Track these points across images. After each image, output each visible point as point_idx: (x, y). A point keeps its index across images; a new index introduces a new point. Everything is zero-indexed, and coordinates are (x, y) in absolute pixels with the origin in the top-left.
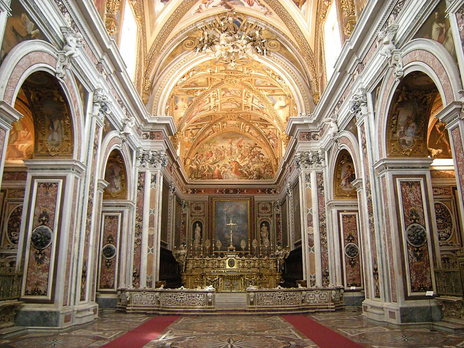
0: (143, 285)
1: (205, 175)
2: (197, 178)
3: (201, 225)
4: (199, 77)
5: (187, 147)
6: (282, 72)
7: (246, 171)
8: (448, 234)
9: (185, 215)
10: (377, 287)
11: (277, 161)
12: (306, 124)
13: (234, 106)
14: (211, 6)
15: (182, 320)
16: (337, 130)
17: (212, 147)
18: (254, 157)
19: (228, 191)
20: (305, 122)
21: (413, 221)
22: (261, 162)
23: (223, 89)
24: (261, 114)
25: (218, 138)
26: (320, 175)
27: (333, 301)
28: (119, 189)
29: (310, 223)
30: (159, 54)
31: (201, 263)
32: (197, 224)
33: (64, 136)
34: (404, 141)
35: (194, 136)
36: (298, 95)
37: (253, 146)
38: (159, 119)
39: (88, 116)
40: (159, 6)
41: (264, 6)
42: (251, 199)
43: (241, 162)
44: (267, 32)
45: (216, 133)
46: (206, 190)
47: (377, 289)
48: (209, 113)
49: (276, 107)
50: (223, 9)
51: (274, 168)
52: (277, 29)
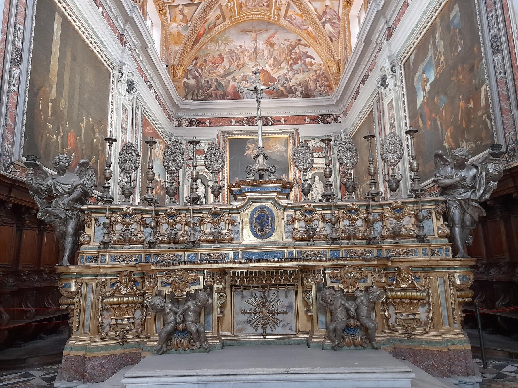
1: (211, 96)
5: (176, 43)
7: (282, 86)
17: (222, 47)
18: (295, 63)
25: (233, 31)
31: (143, 223)
35: (187, 22)
37: (293, 43)
43: (274, 70)
45: (228, 21)
51: (332, 79)
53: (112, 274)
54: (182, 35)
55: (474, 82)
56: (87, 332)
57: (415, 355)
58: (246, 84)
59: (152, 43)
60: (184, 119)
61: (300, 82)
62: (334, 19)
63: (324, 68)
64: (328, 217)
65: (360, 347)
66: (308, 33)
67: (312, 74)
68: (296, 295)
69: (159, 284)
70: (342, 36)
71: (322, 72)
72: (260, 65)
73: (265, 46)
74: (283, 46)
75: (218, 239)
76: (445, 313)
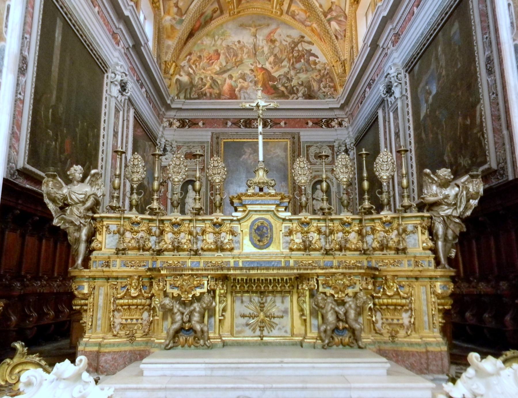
1: (205, 95)
5: (169, 37)
7: (283, 85)
17: (219, 42)
19: (250, 123)
22: (313, 69)
25: (230, 25)
31: (149, 232)
32: (190, 187)
35: (182, 15)
37: (296, 40)
42: (294, 138)
43: (275, 69)
45: (226, 16)
51: (337, 80)
53: (122, 278)
54: (176, 29)
55: (471, 100)
56: (99, 330)
57: (397, 355)
58: (243, 83)
59: (146, 41)
60: (175, 120)
61: (302, 82)
62: (340, 16)
63: (328, 68)
64: (323, 229)
65: (347, 347)
66: (313, 30)
67: (315, 74)
68: (292, 301)
69: (168, 287)
70: (348, 34)
71: (326, 72)
72: (259, 63)
73: (265, 42)
74: (284, 43)
75: (220, 248)
76: (426, 318)
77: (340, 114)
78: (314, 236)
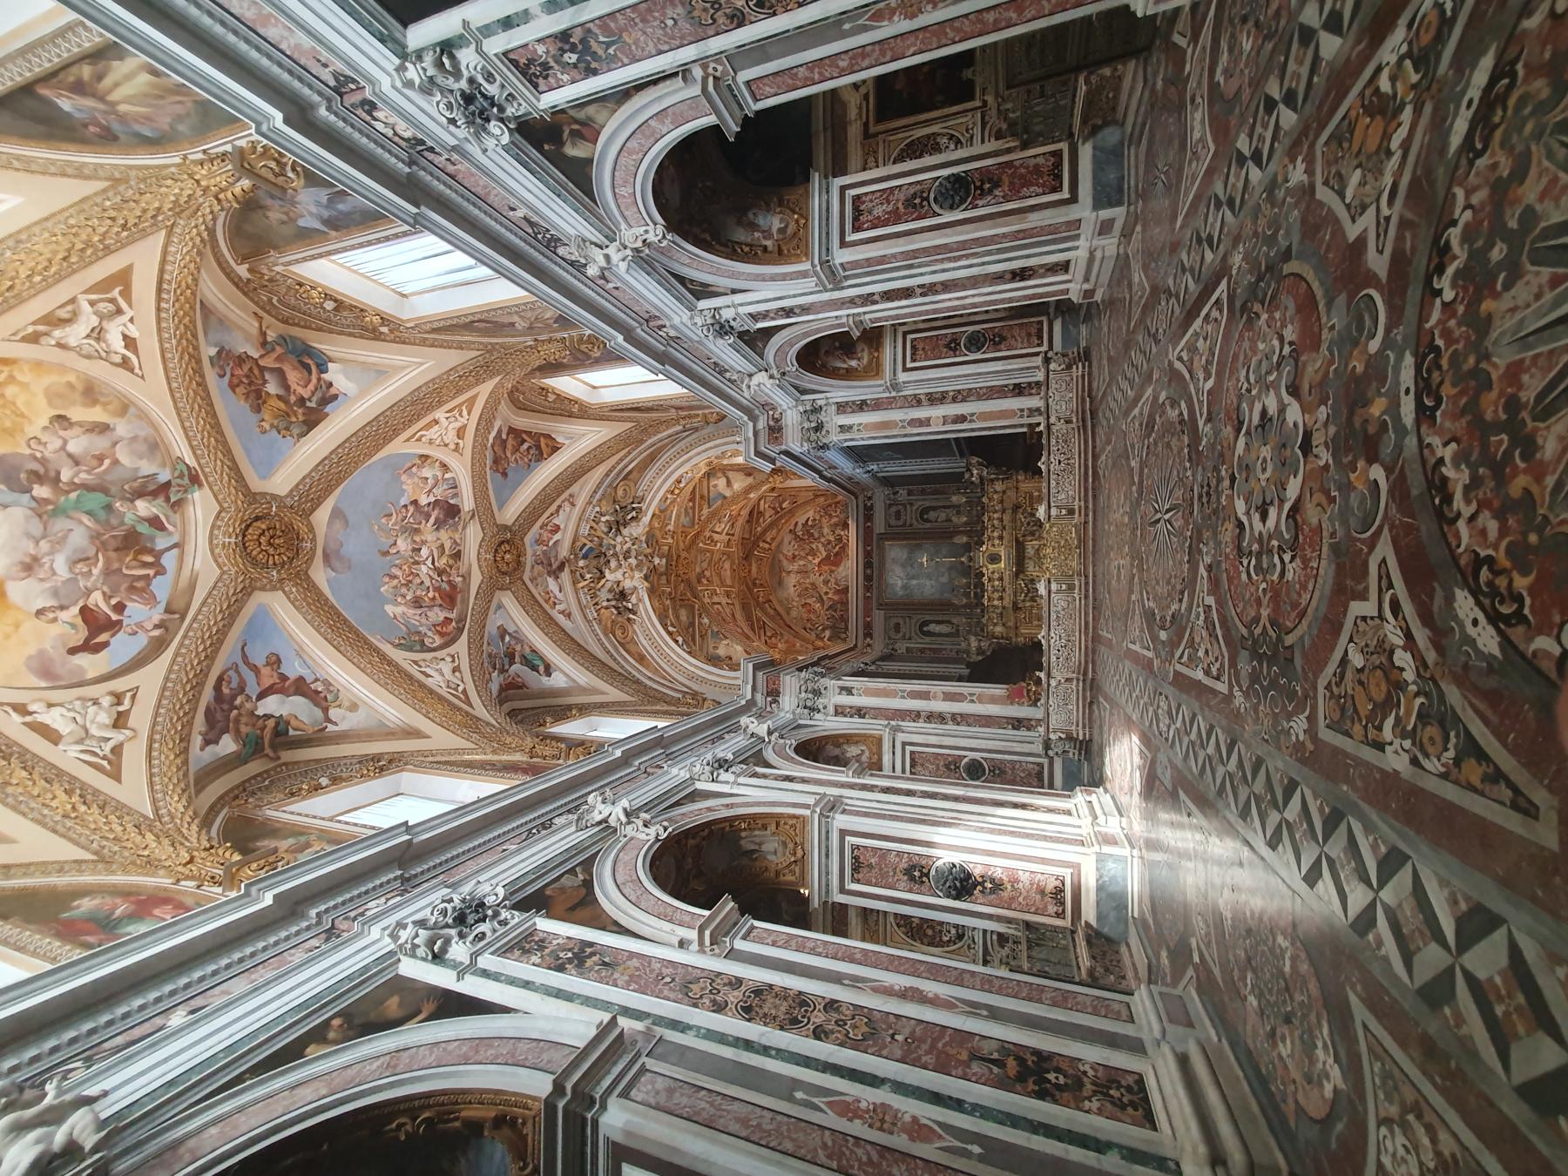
0: (1037, 713)
2: (847, 628)
3: (926, 623)
4: (677, 617)
5: (794, 645)
6: (669, 476)
8: (950, 139)
9: (907, 649)
10: (1048, 270)
11: (817, 496)
12: (756, 434)
13: (727, 565)
14: (559, 595)
15: (1105, 634)
16: (763, 373)
18: (812, 535)
20: (751, 434)
21: (925, 203)
23: (699, 582)
24: (741, 521)
26: (842, 408)
27: (1069, 367)
28: (864, 748)
29: (926, 422)
30: (638, 682)
33: (768, 832)
34: (780, 231)
36: (707, 450)
38: (745, 682)
39: (735, 791)
40: (557, 681)
41: (560, 507)
44: (604, 502)
46: (867, 612)
47: (1053, 269)
48: (738, 607)
49: (728, 493)
50: (565, 576)
51: (829, 501)
52: (598, 487)
75: (1001, 579)
77: (861, 498)
78: (996, 534)
